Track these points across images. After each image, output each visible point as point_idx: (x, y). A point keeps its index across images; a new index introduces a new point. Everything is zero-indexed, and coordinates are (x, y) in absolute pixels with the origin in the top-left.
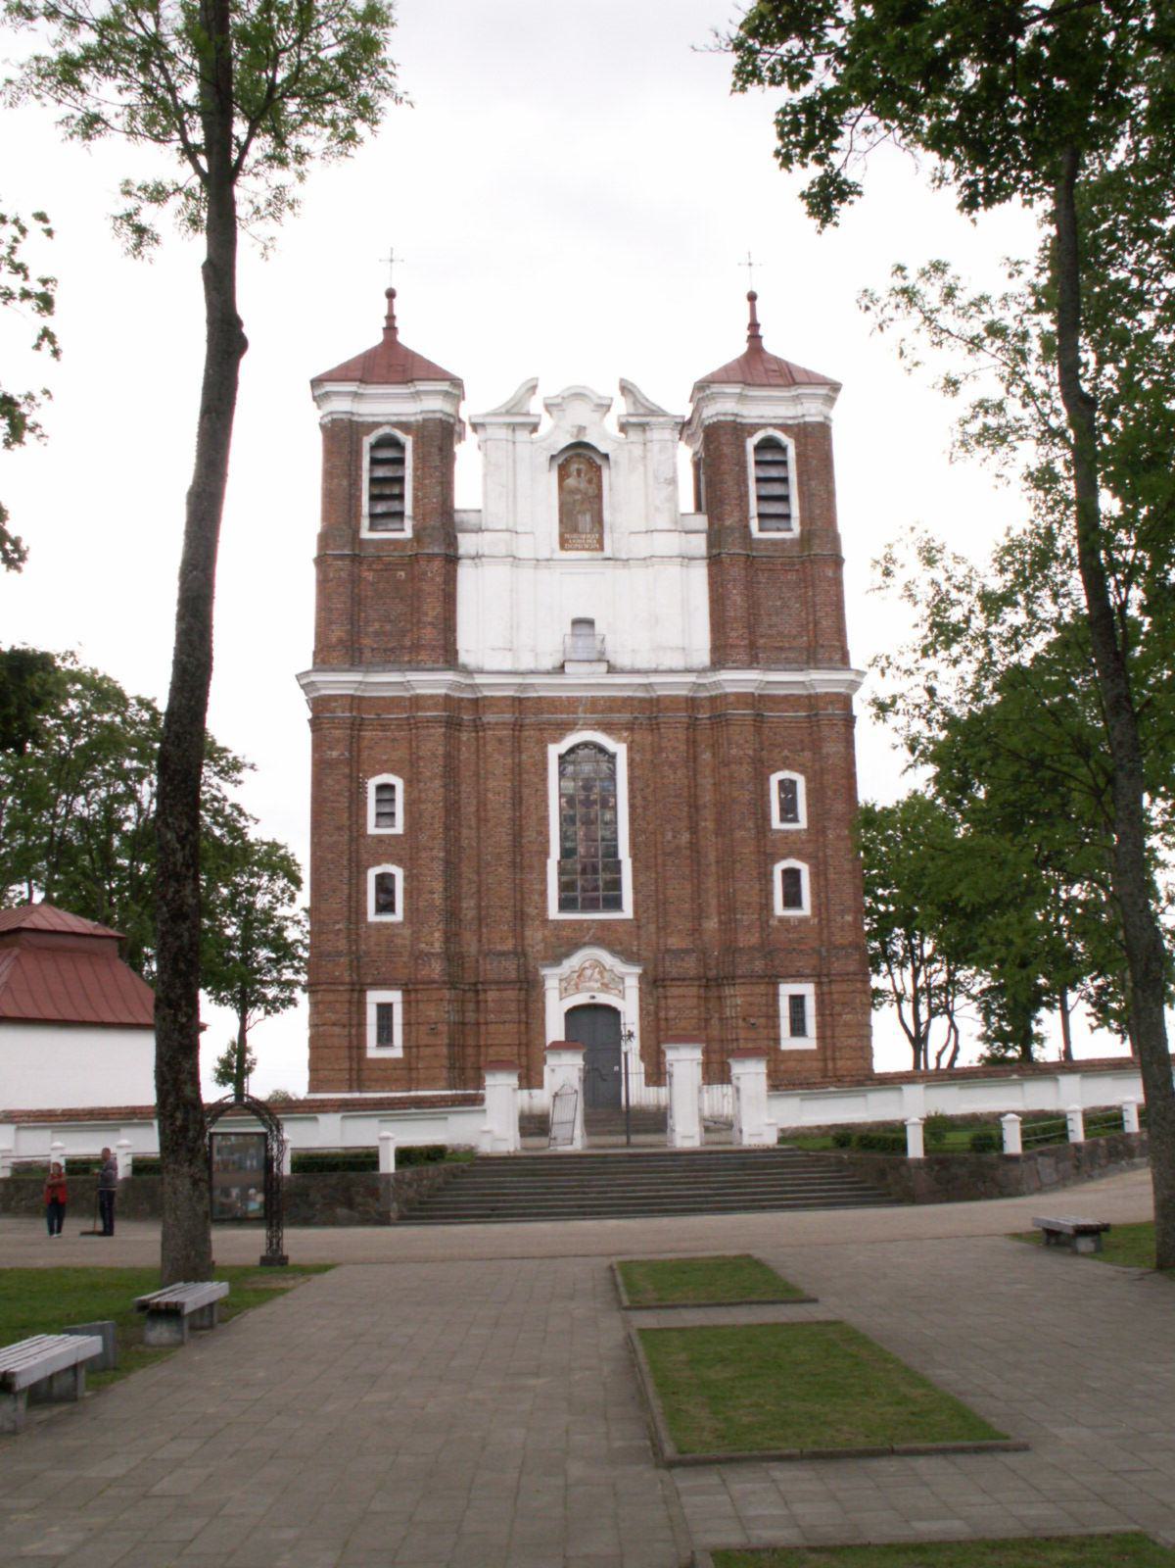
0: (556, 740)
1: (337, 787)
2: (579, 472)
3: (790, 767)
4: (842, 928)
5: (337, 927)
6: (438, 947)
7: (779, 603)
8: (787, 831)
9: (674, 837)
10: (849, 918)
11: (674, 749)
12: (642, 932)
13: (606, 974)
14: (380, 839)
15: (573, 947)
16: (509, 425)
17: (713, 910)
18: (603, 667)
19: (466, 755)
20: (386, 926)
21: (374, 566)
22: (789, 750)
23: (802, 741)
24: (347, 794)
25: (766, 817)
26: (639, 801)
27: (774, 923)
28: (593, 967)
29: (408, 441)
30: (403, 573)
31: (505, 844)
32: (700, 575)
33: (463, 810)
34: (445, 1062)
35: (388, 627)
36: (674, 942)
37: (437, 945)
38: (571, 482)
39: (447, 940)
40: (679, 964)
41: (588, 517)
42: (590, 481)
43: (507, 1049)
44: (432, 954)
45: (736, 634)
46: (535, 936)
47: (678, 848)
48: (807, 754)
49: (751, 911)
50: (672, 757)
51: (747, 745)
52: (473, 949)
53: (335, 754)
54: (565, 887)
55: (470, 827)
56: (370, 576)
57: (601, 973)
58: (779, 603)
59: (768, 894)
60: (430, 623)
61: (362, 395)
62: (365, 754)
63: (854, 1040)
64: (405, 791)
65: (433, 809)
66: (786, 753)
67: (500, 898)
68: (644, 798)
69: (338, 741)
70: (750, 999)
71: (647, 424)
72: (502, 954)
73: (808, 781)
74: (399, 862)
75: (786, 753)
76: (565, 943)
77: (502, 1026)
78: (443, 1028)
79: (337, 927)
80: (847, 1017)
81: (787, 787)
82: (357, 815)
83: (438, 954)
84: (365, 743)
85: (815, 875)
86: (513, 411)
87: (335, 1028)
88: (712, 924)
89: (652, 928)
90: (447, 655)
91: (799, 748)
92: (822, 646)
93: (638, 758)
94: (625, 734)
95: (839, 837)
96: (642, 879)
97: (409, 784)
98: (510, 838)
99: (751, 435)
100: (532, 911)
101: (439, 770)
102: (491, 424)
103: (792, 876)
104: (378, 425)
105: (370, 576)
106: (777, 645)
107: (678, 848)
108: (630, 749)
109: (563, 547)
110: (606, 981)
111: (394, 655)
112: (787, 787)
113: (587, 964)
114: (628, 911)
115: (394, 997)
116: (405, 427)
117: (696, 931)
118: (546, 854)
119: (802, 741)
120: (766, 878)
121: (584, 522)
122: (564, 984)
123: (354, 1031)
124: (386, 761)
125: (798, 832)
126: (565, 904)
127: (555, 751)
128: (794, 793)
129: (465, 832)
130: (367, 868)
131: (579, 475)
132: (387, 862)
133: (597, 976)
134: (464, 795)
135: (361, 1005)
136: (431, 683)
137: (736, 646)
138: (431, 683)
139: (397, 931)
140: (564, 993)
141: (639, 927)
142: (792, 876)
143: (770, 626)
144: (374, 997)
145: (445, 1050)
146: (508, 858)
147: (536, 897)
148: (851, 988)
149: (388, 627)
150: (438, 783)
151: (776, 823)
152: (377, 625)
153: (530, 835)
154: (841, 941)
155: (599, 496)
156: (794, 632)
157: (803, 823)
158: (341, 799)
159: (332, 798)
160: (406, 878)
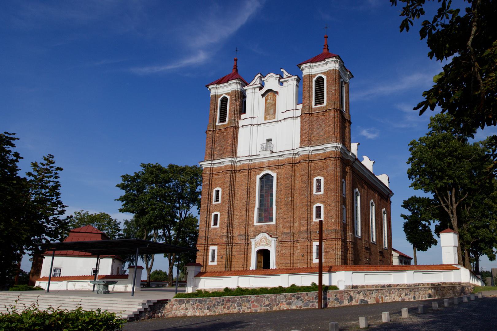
0: (259, 174)
1: (206, 192)
2: (271, 98)
3: (319, 175)
4: (331, 224)
5: (203, 229)
6: (225, 234)
7: (319, 126)
8: (318, 195)
9: (287, 199)
10: (333, 221)
11: (288, 173)
12: (278, 228)
13: (267, 240)
14: (215, 205)
15: (260, 232)
16: (253, 88)
17: (297, 220)
18: (270, 152)
19: (238, 180)
20: (215, 228)
21: (219, 132)
22: (320, 170)
23: (323, 167)
24: (208, 194)
25: (311, 191)
26: (279, 190)
27: (312, 223)
28: (264, 238)
29: (228, 97)
30: (225, 133)
31: (244, 205)
32: (299, 120)
33: (236, 196)
34: (224, 266)
35: (221, 148)
36: (286, 230)
37: (225, 233)
38: (268, 101)
39: (228, 231)
40: (286, 237)
41: (272, 110)
42: (273, 100)
43: (241, 262)
44: (223, 236)
45: (306, 138)
46: (251, 230)
47: (288, 202)
48: (325, 171)
49: (304, 220)
50: (288, 176)
51: (306, 170)
52: (237, 234)
53: (206, 183)
54: (260, 215)
55: (238, 200)
56: (218, 135)
57: (266, 240)
58: (319, 126)
59: (311, 215)
60: (229, 146)
61: (218, 87)
62: (213, 183)
63: (333, 259)
64: (222, 192)
65: (227, 196)
66: (318, 171)
67: (243, 220)
68: (281, 188)
69: (207, 179)
70: (303, 247)
71: (287, 80)
72: (242, 235)
73: (325, 179)
74: (219, 211)
75: (318, 171)
76: (258, 232)
77: (240, 256)
78: (224, 256)
79: (203, 229)
80: (331, 252)
81: (319, 181)
82: (210, 199)
83: (225, 236)
84: (213, 180)
85: (325, 208)
86: (255, 84)
87: (201, 257)
88: (296, 225)
89: (281, 226)
90: (234, 153)
91: (322, 169)
92: (329, 137)
93: (279, 177)
94: (276, 170)
95: (331, 195)
96: (279, 212)
97: (223, 189)
98: (246, 202)
99: (314, 77)
100: (250, 222)
101: (228, 185)
102: (249, 89)
103: (319, 208)
104: (222, 95)
105: (218, 135)
106: (318, 139)
107: (288, 202)
108: (277, 174)
109: (265, 120)
110: (267, 242)
111: (222, 156)
112: (319, 181)
113: (262, 238)
114: (274, 222)
115: (215, 248)
116: (228, 94)
117: (292, 226)
118: (254, 206)
119: (323, 167)
120: (311, 209)
121: (271, 111)
122: (256, 243)
123: (205, 257)
124: (218, 184)
125: (321, 195)
126: (260, 221)
127: (259, 177)
128: (320, 183)
129: (236, 202)
130: (212, 213)
131: (270, 99)
132: (217, 211)
133: (265, 241)
134: (236, 192)
135: (207, 250)
136: (227, 161)
137: (305, 141)
138: (227, 161)
139: (218, 230)
140: (256, 246)
141: (277, 226)
142: (319, 208)
143: (316, 133)
144: (211, 248)
145: (224, 263)
146: (245, 208)
147: (252, 219)
148: (332, 243)
149: (221, 148)
150: (228, 189)
151: (315, 192)
152: (219, 148)
153: (251, 201)
154: (330, 228)
155: (275, 104)
156: (323, 134)
157: (322, 192)
158: (206, 195)
159: (204, 195)
160: (220, 215)
